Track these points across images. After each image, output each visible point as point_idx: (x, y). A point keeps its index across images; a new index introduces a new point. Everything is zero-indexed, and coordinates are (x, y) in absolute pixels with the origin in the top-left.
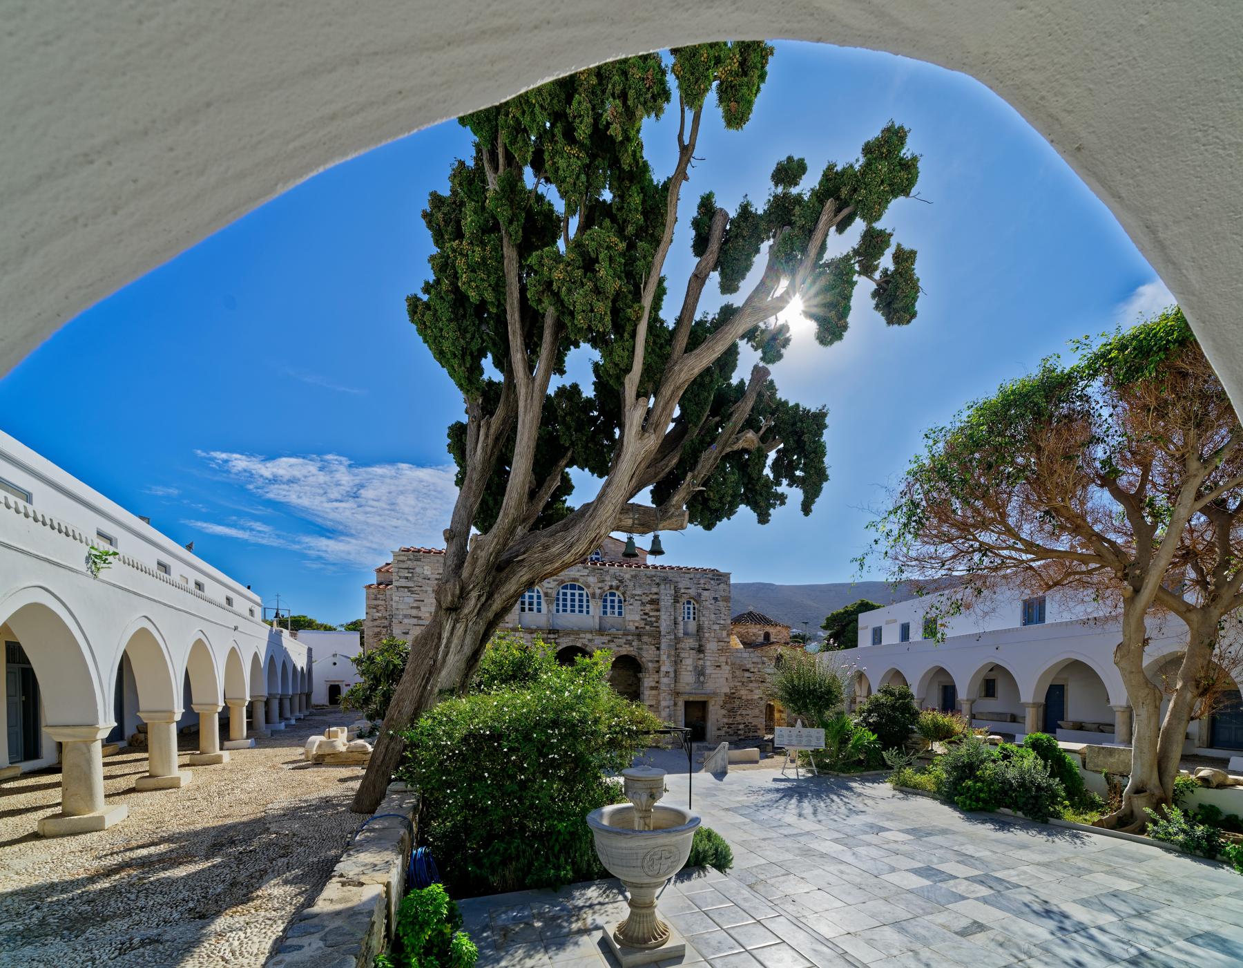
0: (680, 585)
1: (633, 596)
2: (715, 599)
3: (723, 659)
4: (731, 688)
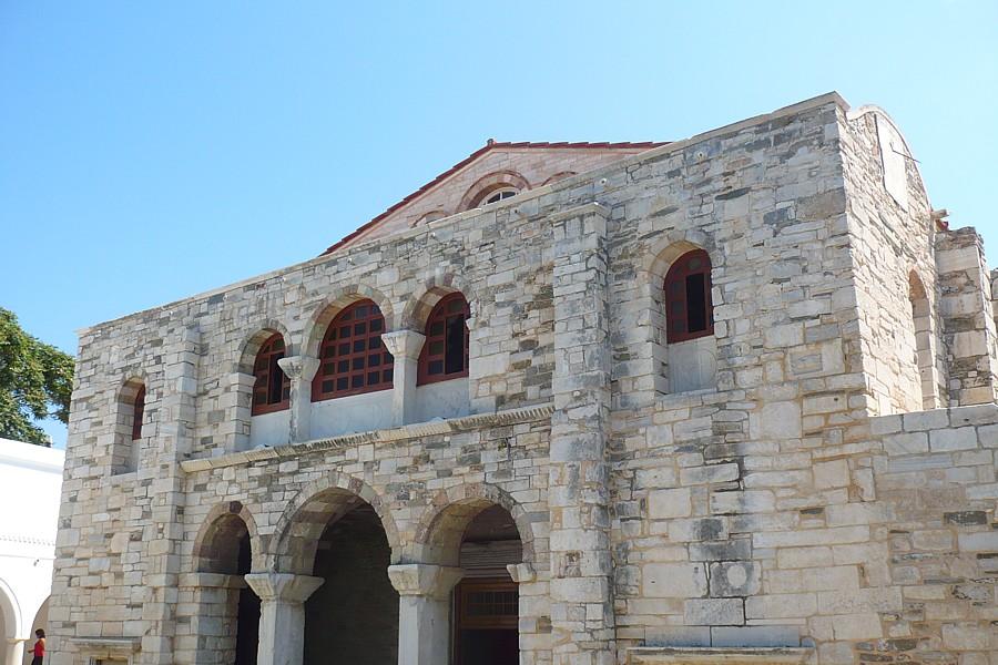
0: (636, 211)
1: (489, 296)
2: (778, 220)
3: (835, 474)
4: (891, 618)
